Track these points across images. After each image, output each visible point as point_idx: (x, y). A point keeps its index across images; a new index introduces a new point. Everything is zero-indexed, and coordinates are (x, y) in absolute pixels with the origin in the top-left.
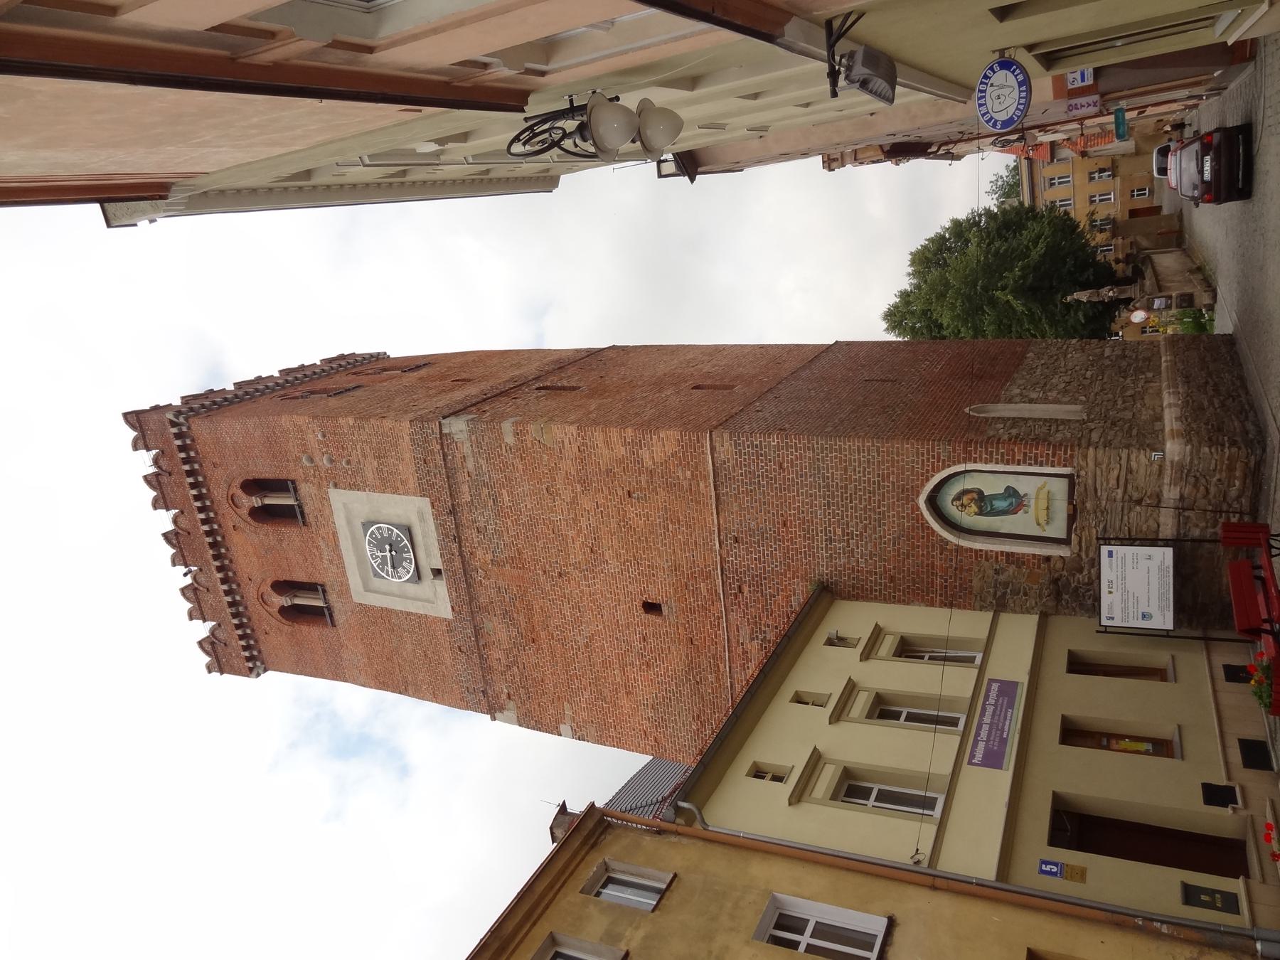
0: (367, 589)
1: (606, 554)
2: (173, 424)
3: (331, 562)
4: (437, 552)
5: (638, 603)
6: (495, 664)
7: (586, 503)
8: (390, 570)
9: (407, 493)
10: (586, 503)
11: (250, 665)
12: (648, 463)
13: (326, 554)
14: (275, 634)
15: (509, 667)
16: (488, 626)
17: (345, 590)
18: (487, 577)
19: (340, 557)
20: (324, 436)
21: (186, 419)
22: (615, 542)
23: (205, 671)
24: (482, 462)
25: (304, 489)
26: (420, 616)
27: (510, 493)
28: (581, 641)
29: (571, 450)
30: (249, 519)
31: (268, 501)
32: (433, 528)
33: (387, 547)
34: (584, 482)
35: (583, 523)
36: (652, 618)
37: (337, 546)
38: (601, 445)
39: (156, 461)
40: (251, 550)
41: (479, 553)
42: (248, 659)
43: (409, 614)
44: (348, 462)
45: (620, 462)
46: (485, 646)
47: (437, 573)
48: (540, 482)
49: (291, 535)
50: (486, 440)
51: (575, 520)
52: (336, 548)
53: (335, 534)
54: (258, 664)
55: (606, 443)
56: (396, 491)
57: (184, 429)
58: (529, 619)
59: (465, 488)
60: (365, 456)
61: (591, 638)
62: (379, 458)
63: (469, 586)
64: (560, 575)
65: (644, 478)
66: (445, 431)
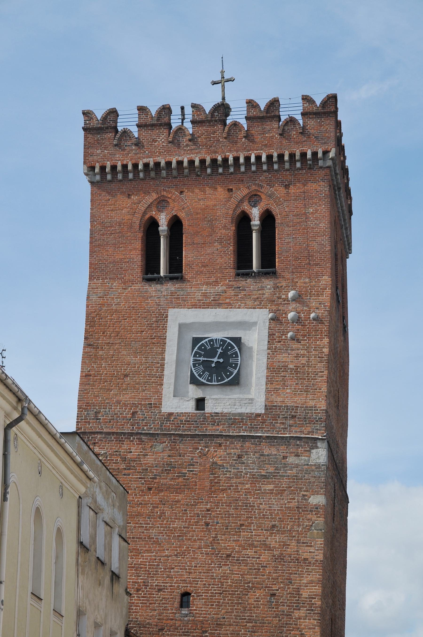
0: (182, 327)
1: (227, 568)
2: (325, 153)
3: (205, 295)
4: (219, 410)
5: (189, 589)
6: (125, 446)
7: (265, 556)
8: (201, 359)
9: (268, 392)
10: (265, 556)
11: (97, 170)
12: (296, 614)
13: (212, 290)
14: (131, 208)
15: (124, 459)
16: (159, 447)
17: (180, 302)
18: (203, 455)
19: (207, 306)
20: (314, 319)
21: (329, 167)
22: (236, 577)
23: (86, 108)
24: (295, 470)
25: (268, 284)
26: (161, 377)
27: (271, 492)
28: (153, 532)
29: (305, 553)
30: (239, 211)
31: (254, 235)
32: (239, 411)
33: (221, 360)
34: (280, 559)
35: (250, 552)
36: (178, 599)
37: (219, 305)
38: (310, 578)
39: (292, 121)
40: (211, 203)
41: (221, 452)
42: (103, 168)
43: (163, 365)
44: (292, 339)
45: (298, 590)
46: (140, 439)
47: (200, 403)
48: (281, 520)
49: (227, 257)
50: (312, 480)
51: (252, 546)
52: (217, 303)
53: (229, 306)
54: (98, 178)
55: (311, 582)
56: (269, 381)
57: (321, 163)
58: (169, 488)
59: (274, 451)
60: (298, 356)
61: (157, 542)
62: (297, 372)
63: (193, 436)
64: (207, 524)
65: (286, 608)
66: (319, 444)
